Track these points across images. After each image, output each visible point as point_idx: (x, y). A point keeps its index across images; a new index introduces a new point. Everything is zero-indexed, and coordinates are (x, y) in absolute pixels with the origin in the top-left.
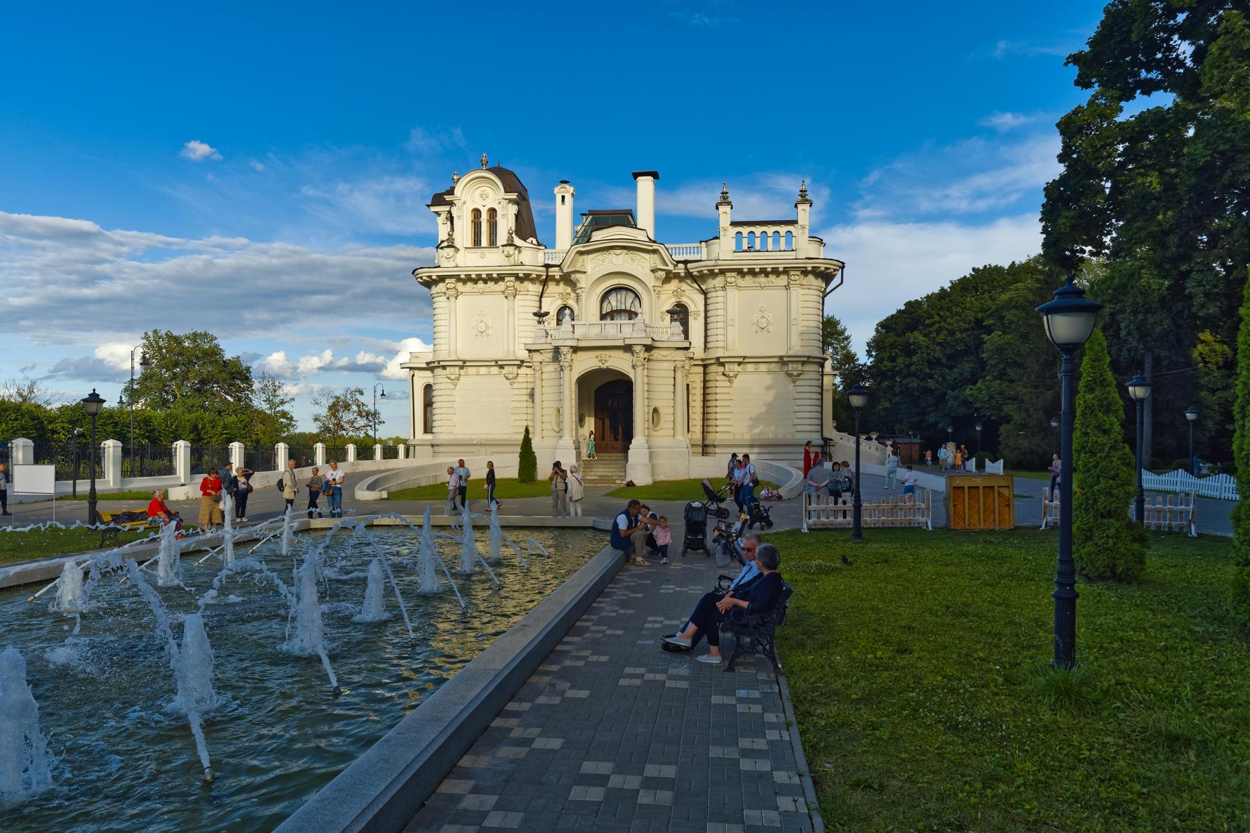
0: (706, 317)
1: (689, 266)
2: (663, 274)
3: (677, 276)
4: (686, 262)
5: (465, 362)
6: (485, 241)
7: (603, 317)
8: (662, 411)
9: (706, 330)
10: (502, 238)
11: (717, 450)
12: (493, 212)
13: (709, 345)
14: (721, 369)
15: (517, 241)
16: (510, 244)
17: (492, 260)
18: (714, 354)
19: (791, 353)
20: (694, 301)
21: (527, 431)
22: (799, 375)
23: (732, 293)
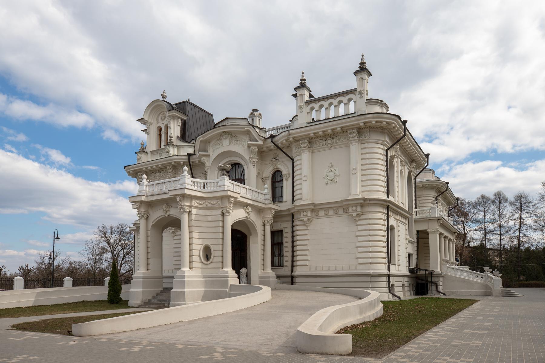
4: (272, 137)
13: (295, 198)
20: (285, 168)
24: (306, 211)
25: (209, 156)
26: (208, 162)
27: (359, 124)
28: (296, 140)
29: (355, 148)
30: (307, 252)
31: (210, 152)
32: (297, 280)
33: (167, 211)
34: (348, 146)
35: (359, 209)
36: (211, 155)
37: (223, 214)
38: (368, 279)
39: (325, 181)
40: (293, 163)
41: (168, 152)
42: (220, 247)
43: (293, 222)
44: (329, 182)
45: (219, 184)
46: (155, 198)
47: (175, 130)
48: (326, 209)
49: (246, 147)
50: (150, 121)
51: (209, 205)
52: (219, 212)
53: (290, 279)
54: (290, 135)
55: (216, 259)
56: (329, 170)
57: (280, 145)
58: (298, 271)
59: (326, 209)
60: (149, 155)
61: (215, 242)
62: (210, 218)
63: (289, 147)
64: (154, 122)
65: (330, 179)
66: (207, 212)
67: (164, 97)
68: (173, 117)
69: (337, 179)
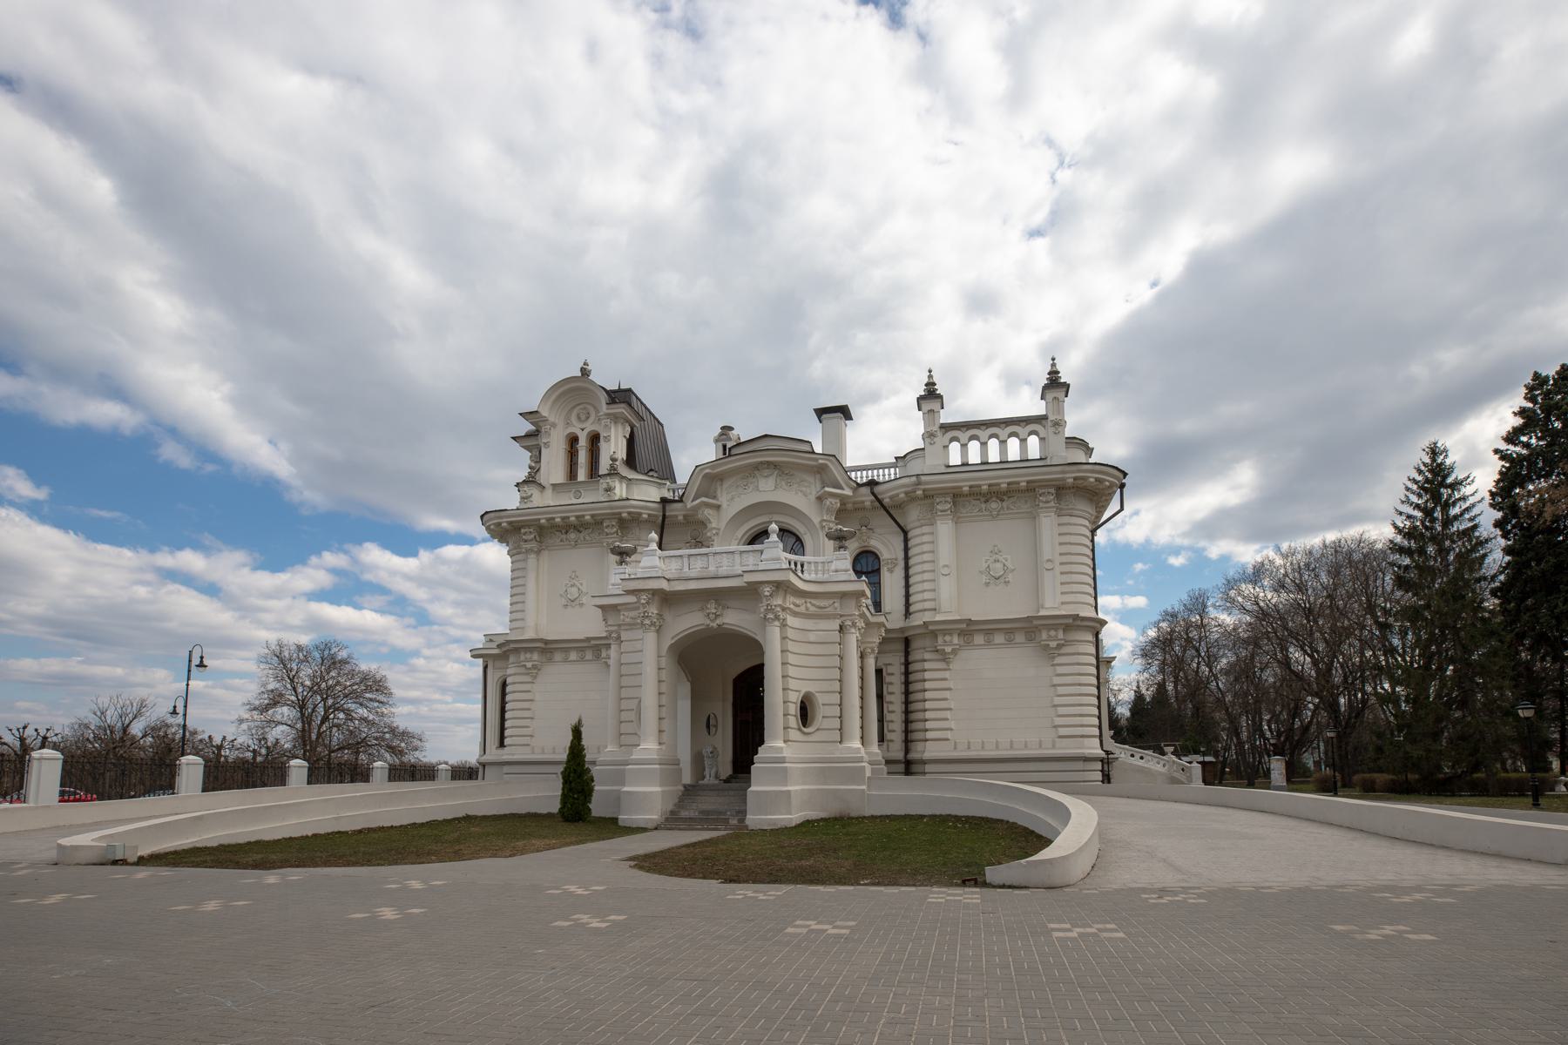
0: (907, 568)
1: (877, 489)
3: (859, 508)
4: (872, 483)
5: (546, 642)
6: (582, 475)
8: (820, 699)
9: (907, 586)
10: (604, 466)
11: (928, 768)
12: (595, 439)
13: (912, 609)
14: (928, 642)
15: (624, 471)
16: (613, 472)
17: (590, 498)
18: (917, 620)
20: (887, 547)
21: (577, 732)
22: (1059, 646)
23: (945, 529)
24: (949, 632)
25: (718, 507)
26: (717, 522)
27: (1063, 479)
28: (929, 496)
29: (1048, 523)
30: (948, 714)
31: (723, 499)
32: (915, 768)
33: (717, 616)
34: (1034, 517)
35: (1061, 635)
36: (724, 506)
37: (841, 629)
38: (1080, 765)
39: (984, 579)
40: (906, 540)
41: (609, 489)
42: (836, 698)
43: (907, 653)
45: (833, 567)
46: (693, 585)
47: (614, 446)
48: (989, 633)
49: (813, 497)
50: (551, 419)
51: (812, 609)
52: (836, 625)
53: (901, 767)
54: (919, 483)
55: (826, 724)
57: (886, 501)
58: (929, 751)
59: (989, 633)
60: (549, 492)
61: (825, 686)
62: (812, 637)
63: (874, 508)
64: (561, 425)
66: (809, 624)
68: (615, 418)
69: (1010, 577)
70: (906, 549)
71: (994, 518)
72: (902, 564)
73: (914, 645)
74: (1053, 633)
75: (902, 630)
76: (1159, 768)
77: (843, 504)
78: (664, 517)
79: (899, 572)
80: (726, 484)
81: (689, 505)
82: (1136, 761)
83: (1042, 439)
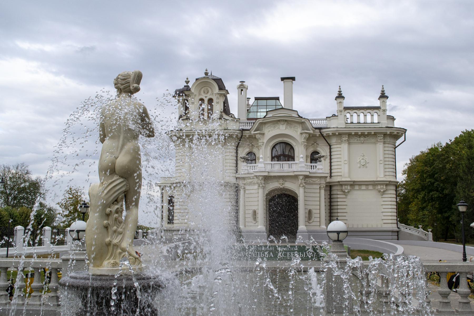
0: (331, 159)
2: (307, 136)
4: (320, 129)
7: (273, 158)
8: (314, 211)
9: (331, 166)
13: (333, 175)
14: (339, 188)
18: (335, 179)
19: (379, 179)
20: (323, 150)
23: (345, 146)
24: (345, 185)
29: (380, 146)
33: (283, 184)
39: (359, 165)
40: (330, 149)
44: (361, 166)
49: (299, 133)
50: (195, 93)
52: (318, 187)
55: (315, 220)
56: (361, 158)
57: (325, 135)
64: (197, 95)
65: (363, 164)
67: (206, 74)
70: (330, 152)
71: (363, 143)
72: (329, 157)
73: (334, 188)
74: (382, 186)
75: (329, 183)
76: (416, 234)
77: (309, 136)
78: (242, 136)
79: (328, 160)
80: (267, 126)
81: (253, 132)
82: (407, 231)
83: (379, 115)
